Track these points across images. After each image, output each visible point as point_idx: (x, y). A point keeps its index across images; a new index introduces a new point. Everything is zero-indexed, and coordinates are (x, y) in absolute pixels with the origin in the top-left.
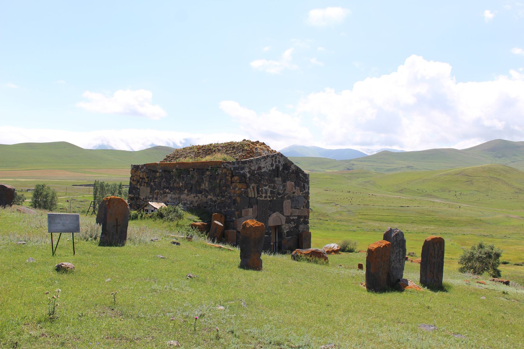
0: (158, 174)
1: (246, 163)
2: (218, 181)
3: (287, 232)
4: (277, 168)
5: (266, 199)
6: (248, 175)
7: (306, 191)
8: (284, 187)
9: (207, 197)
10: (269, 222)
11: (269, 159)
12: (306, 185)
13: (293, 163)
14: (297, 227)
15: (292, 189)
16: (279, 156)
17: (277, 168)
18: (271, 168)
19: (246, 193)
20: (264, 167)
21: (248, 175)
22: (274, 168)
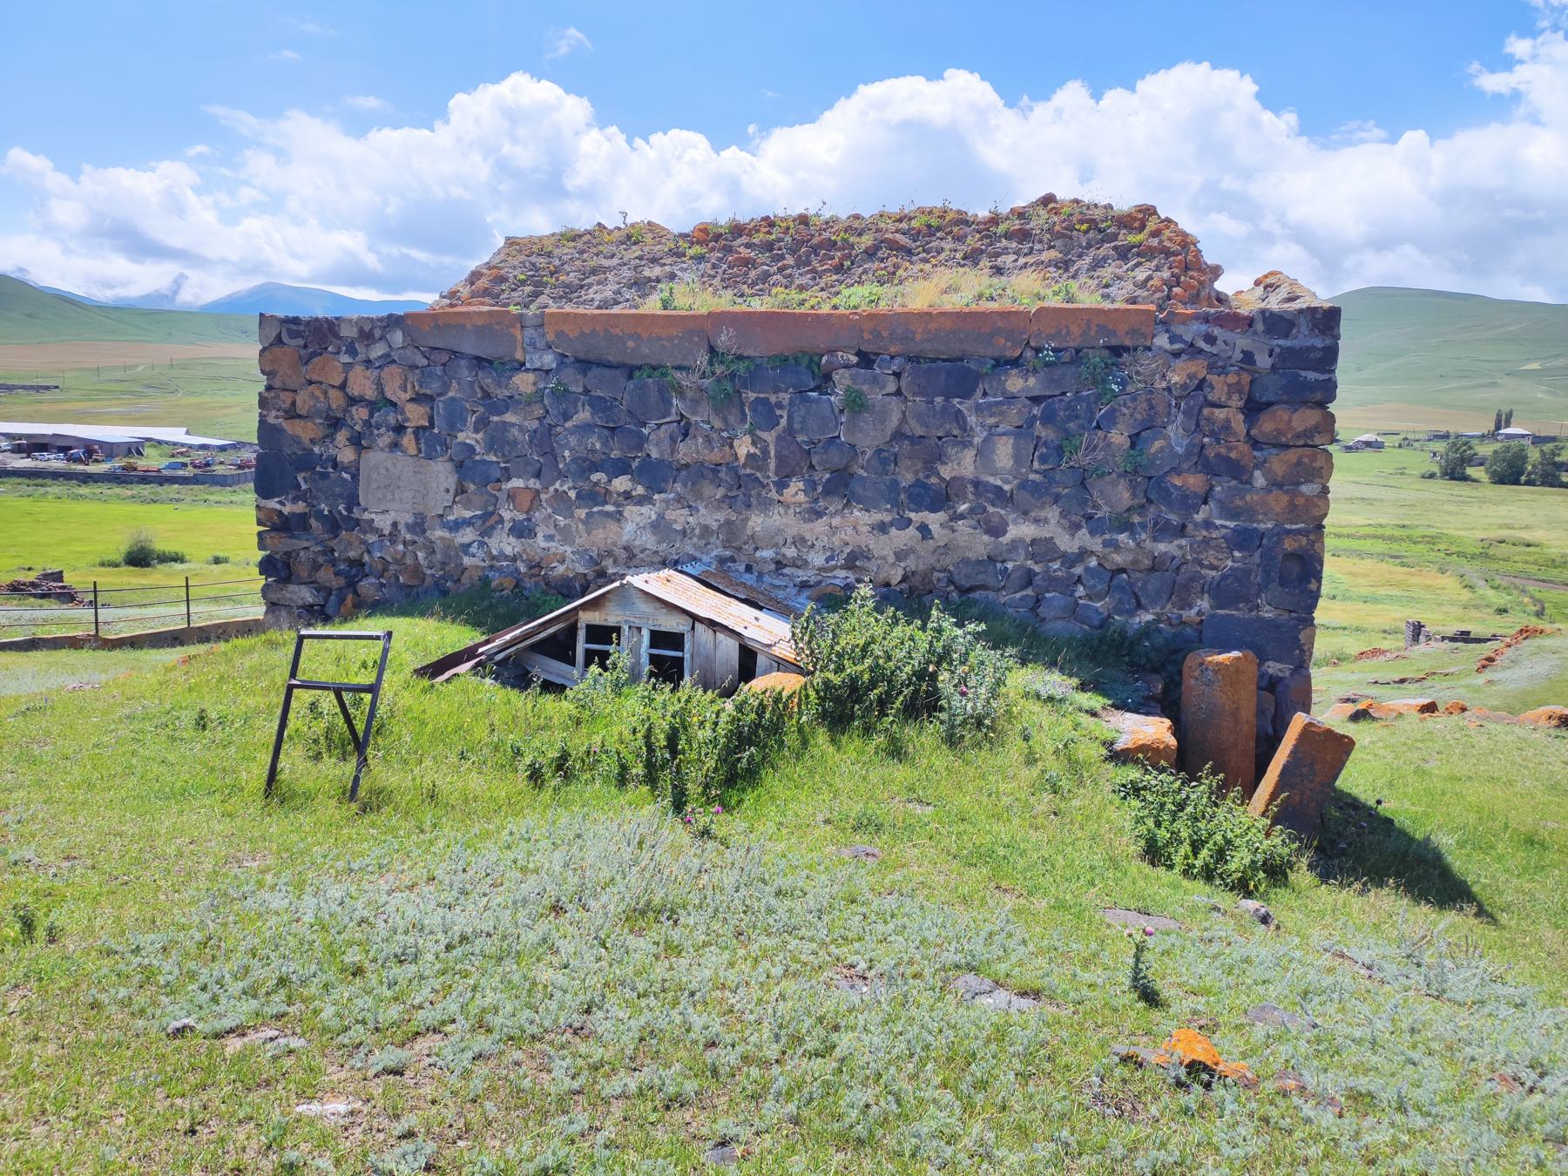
0: (524, 382)
2: (1118, 437)
9: (997, 530)
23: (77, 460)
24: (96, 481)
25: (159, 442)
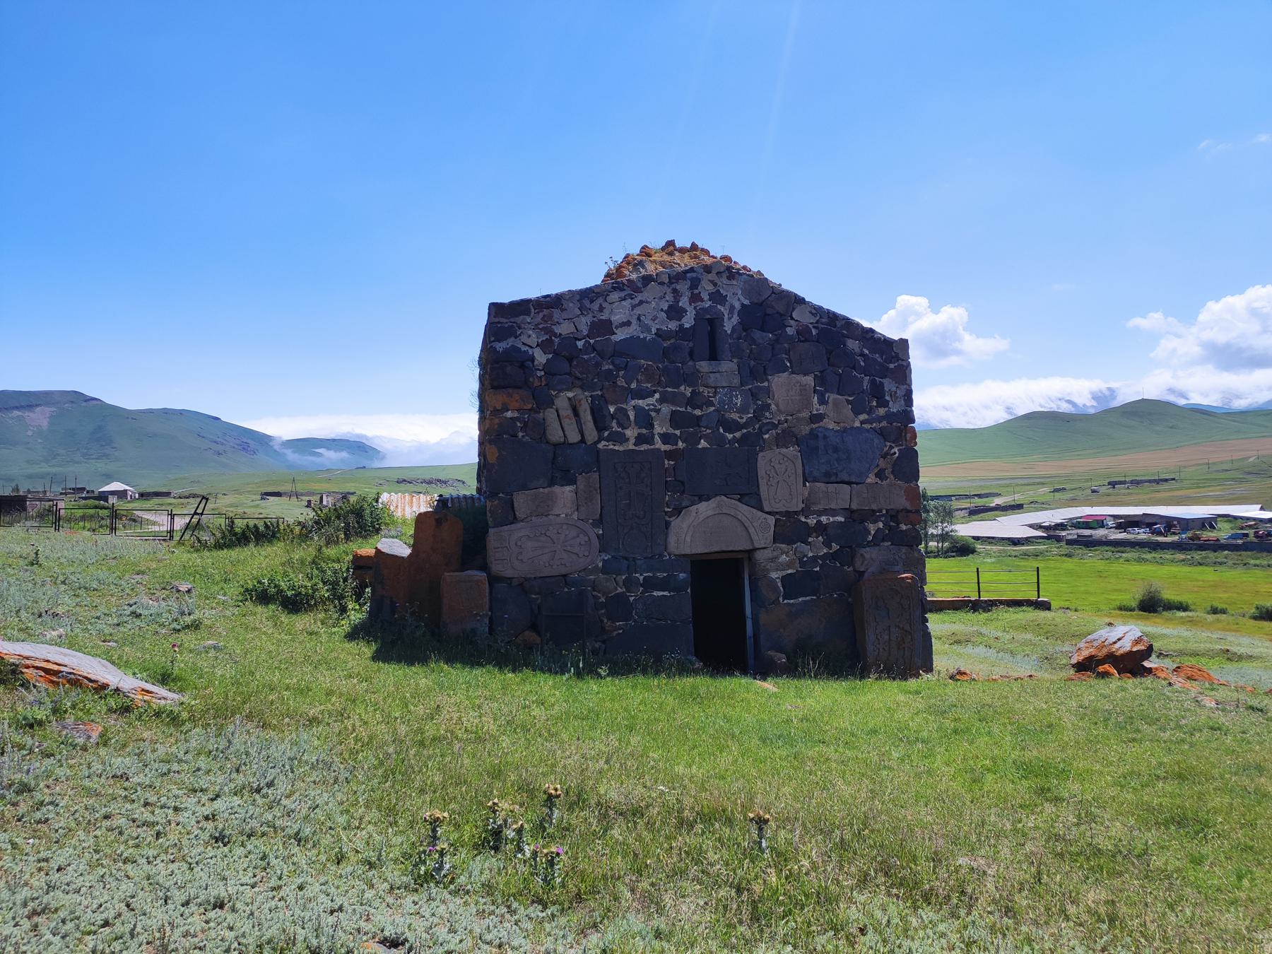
1: (528, 314)
3: (783, 579)
4: (710, 323)
5: (644, 447)
6: (541, 357)
7: (895, 408)
8: (754, 395)
10: (672, 540)
11: (653, 291)
12: (889, 385)
13: (801, 301)
14: (847, 554)
15: (808, 404)
16: (712, 276)
17: (710, 323)
18: (673, 325)
19: (540, 428)
20: (628, 324)
21: (541, 357)
22: (688, 321)
23: (1159, 533)
24: (1162, 549)
25: (1236, 518)
